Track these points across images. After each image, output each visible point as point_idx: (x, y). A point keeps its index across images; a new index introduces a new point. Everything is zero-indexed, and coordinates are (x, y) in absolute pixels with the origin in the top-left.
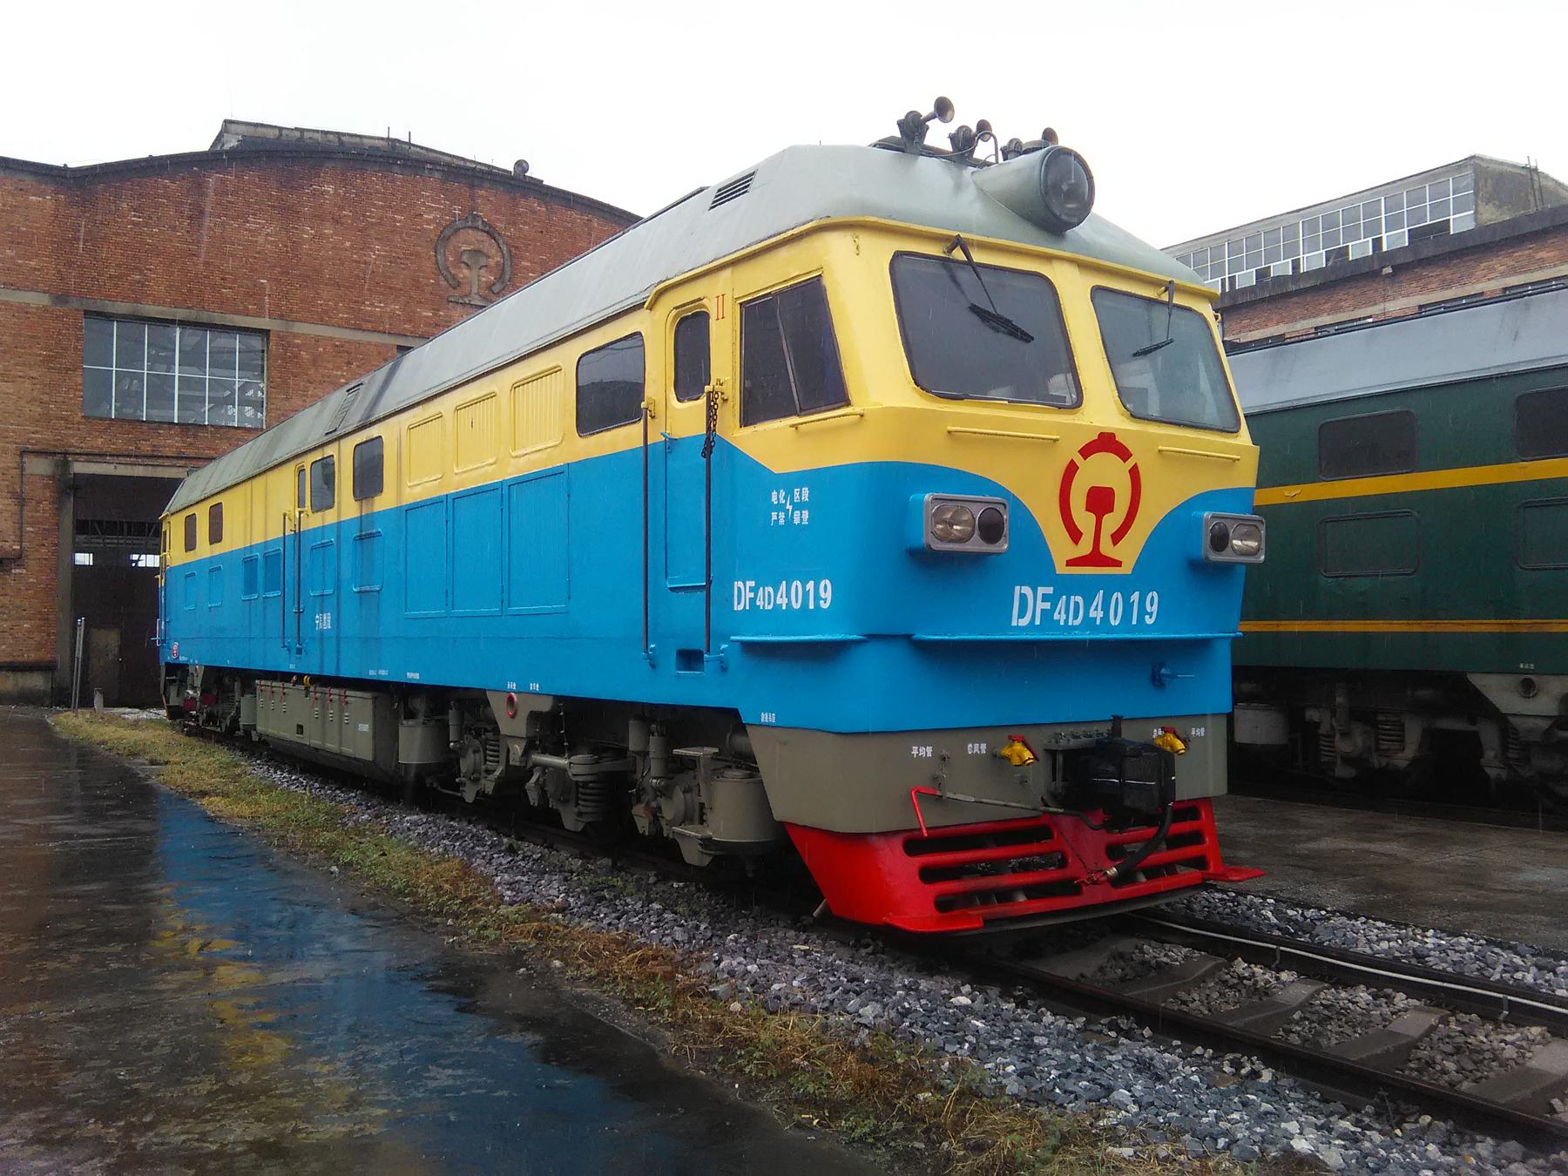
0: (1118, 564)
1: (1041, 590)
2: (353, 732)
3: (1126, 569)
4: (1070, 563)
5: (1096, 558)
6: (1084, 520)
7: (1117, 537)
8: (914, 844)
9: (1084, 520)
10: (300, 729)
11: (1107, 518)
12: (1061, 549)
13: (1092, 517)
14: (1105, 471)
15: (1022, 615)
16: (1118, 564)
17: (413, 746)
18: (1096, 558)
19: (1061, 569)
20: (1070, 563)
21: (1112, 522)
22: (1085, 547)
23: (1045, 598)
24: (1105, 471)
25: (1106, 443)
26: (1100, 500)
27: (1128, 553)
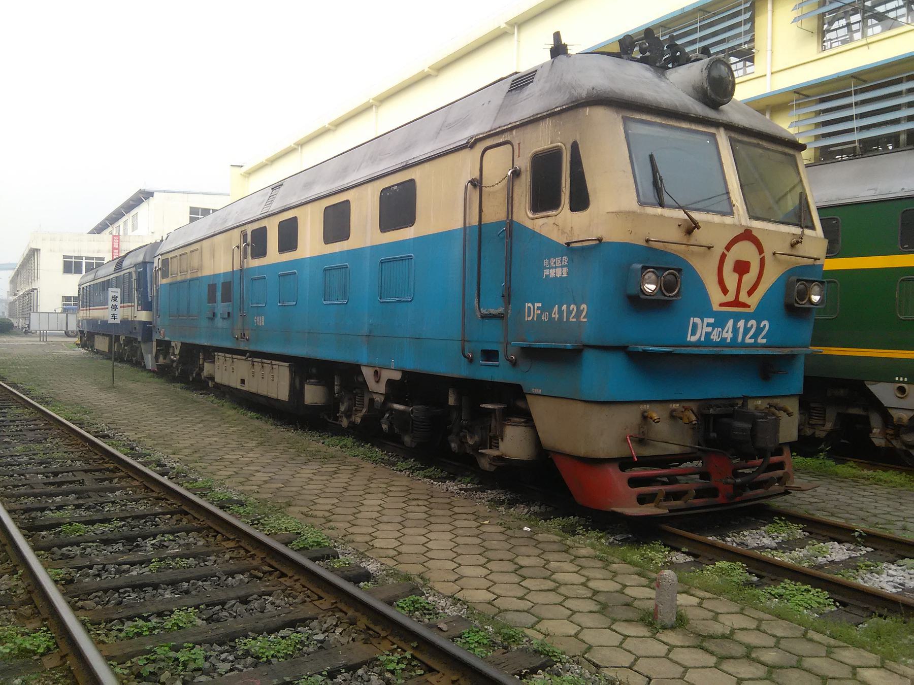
0: (749, 306)
1: (706, 320)
2: (276, 384)
3: (751, 310)
4: (721, 305)
6: (731, 280)
7: (750, 293)
8: (625, 463)
9: (731, 280)
10: (243, 381)
11: (746, 277)
12: (716, 297)
13: (736, 276)
14: (745, 251)
15: (693, 334)
16: (749, 306)
17: (313, 394)
18: (736, 303)
19: (716, 307)
20: (721, 305)
22: (731, 297)
23: (708, 325)
24: (745, 251)
25: (747, 235)
26: (742, 268)
27: (754, 301)
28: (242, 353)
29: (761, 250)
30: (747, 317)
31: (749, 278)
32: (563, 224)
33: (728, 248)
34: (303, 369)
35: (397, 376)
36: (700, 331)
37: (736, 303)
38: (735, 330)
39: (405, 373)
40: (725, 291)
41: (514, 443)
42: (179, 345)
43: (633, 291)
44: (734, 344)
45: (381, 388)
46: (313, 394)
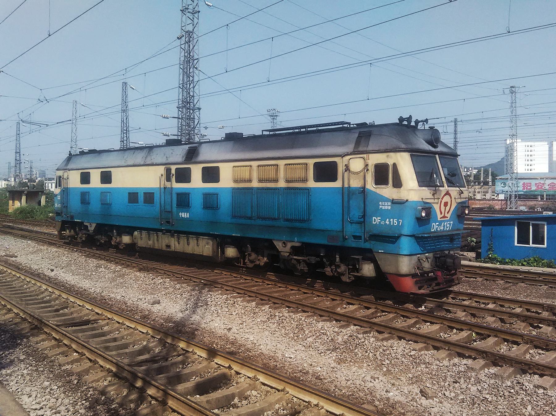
2: (205, 248)
3: (448, 219)
5: (444, 217)
7: (448, 213)
12: (439, 216)
14: (447, 199)
17: (231, 252)
18: (444, 217)
19: (439, 219)
21: (448, 208)
22: (443, 215)
24: (447, 199)
26: (446, 204)
27: (449, 216)
28: (168, 231)
29: (451, 198)
30: (447, 221)
31: (448, 208)
32: (388, 191)
35: (297, 244)
36: (435, 227)
38: (444, 227)
40: (441, 213)
41: (368, 270)
42: (94, 225)
43: (419, 216)
44: (443, 231)
46: (231, 252)
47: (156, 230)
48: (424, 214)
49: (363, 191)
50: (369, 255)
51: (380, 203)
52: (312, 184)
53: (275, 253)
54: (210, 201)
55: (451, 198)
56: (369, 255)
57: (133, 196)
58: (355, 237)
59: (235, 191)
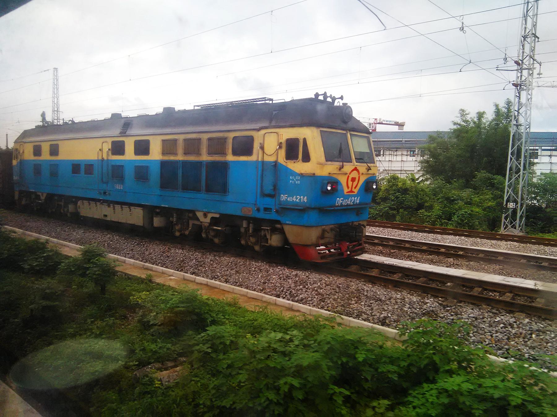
2: (136, 217)
3: (356, 193)
6: (350, 183)
7: (355, 188)
9: (350, 183)
12: (346, 190)
14: (355, 174)
17: (158, 222)
18: (352, 191)
22: (350, 189)
24: (355, 174)
26: (353, 180)
27: (356, 191)
29: (359, 174)
33: (350, 174)
34: (151, 211)
37: (352, 191)
39: (221, 215)
40: (348, 188)
42: (45, 195)
45: (208, 220)
47: (99, 200)
48: (329, 188)
49: (276, 164)
50: (278, 226)
51: (291, 177)
52: (230, 158)
53: (198, 223)
54: (142, 173)
55: (359, 174)
56: (278, 226)
57: (76, 167)
58: (266, 209)
59: (163, 164)
